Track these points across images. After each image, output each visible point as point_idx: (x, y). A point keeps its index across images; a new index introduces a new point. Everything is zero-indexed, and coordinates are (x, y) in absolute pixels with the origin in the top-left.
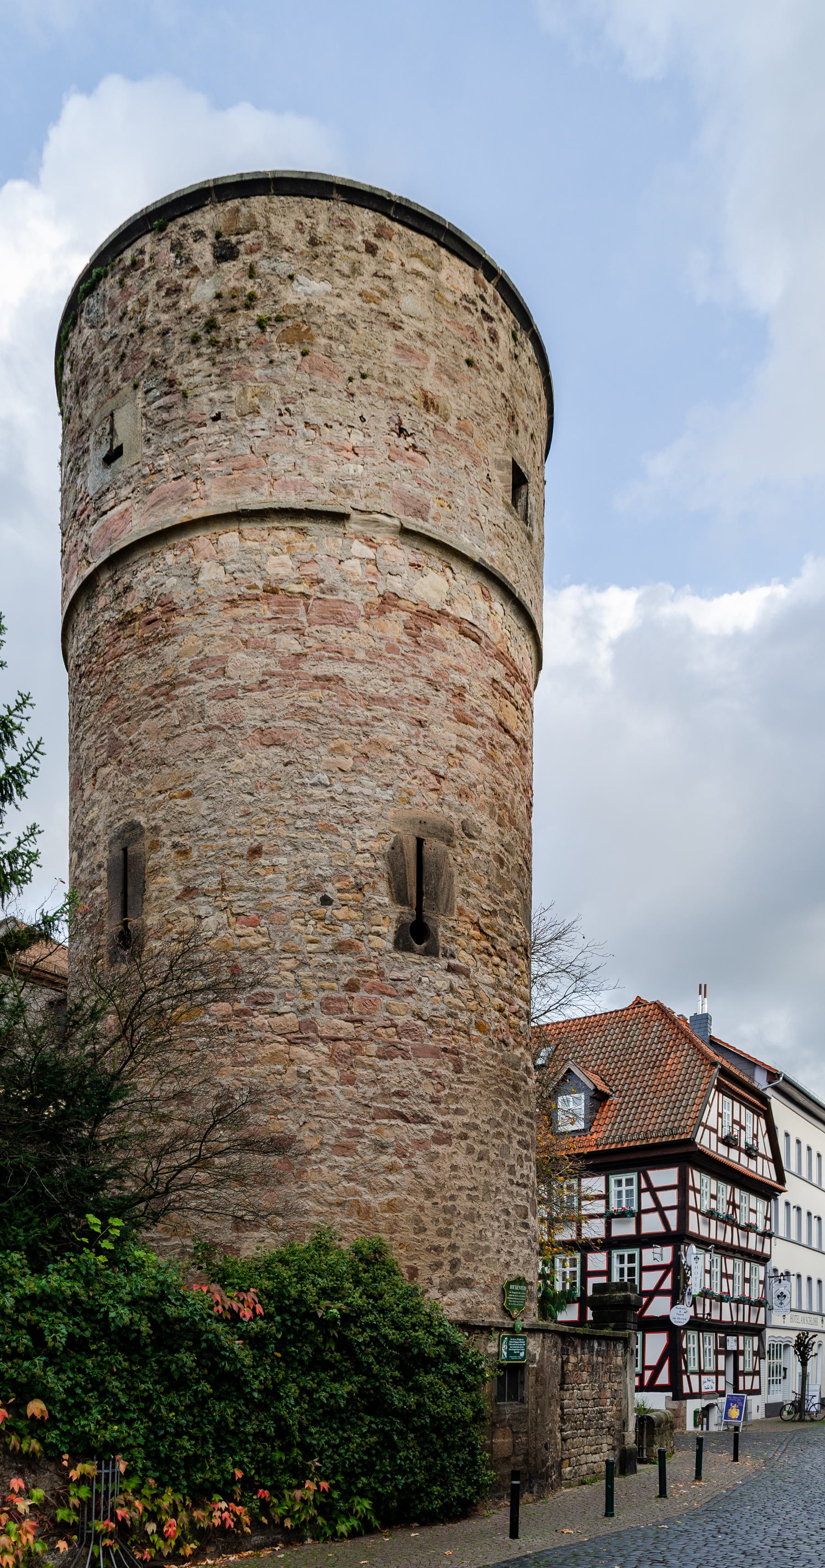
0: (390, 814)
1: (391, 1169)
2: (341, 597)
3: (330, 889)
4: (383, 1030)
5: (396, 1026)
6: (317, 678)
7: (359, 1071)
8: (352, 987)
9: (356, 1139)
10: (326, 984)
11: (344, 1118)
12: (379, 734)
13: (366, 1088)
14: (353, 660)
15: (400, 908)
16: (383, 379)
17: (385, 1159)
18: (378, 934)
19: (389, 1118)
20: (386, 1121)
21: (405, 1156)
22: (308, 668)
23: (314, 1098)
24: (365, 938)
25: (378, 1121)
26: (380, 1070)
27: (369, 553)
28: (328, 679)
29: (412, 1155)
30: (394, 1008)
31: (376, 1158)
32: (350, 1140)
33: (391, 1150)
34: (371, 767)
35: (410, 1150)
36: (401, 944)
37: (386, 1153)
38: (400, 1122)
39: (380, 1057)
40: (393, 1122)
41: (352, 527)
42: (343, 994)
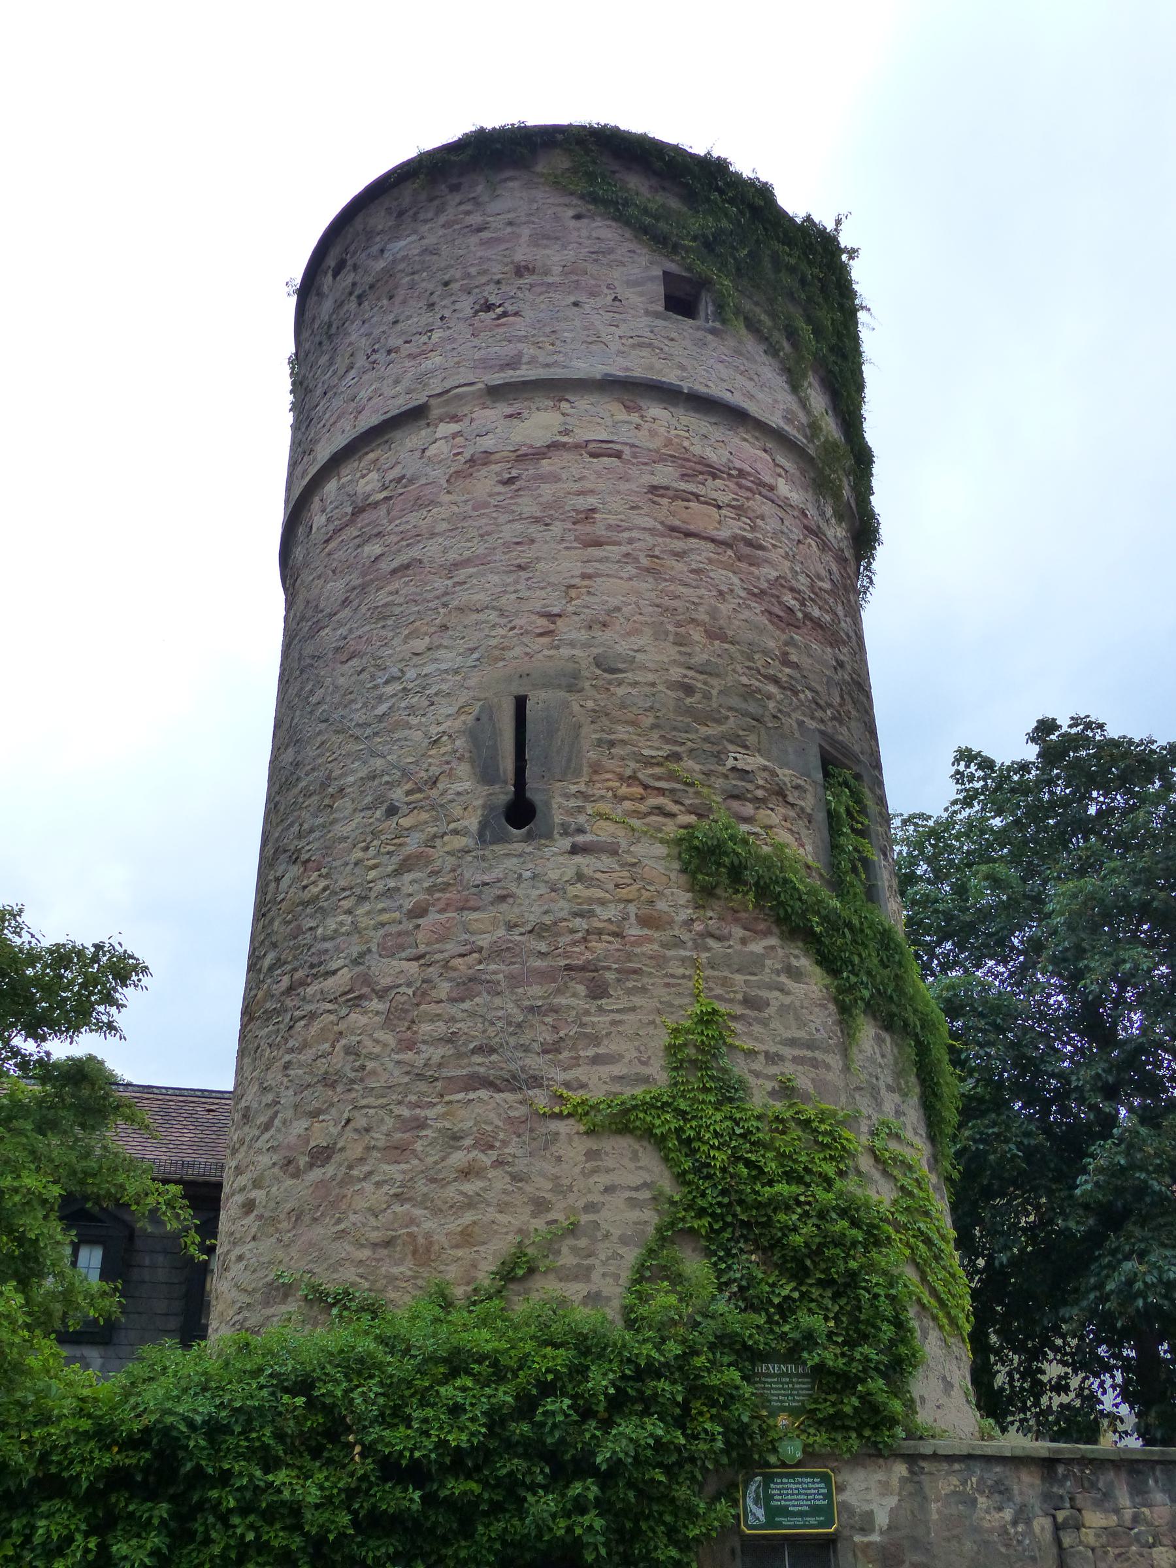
1: (466, 1173)
2: (423, 481)
3: (398, 795)
4: (460, 960)
5: (480, 950)
6: (394, 572)
7: (425, 1028)
8: (419, 912)
9: (415, 1133)
10: (385, 917)
11: (400, 1103)
12: (462, 597)
13: (431, 1050)
14: (433, 535)
15: (484, 790)
16: (468, 276)
17: (458, 1158)
18: (455, 832)
19: (467, 1089)
21: (492, 1147)
22: (385, 566)
23: (362, 1080)
24: (438, 842)
25: (447, 1098)
26: (453, 1019)
27: (454, 427)
28: (407, 567)
29: (505, 1143)
30: (475, 926)
31: (443, 1159)
32: (406, 1136)
33: (468, 1142)
34: (451, 637)
35: (502, 1136)
36: (487, 835)
37: (459, 1148)
38: (483, 1094)
39: (453, 1000)
40: (472, 1095)
41: (435, 413)
42: (408, 925)
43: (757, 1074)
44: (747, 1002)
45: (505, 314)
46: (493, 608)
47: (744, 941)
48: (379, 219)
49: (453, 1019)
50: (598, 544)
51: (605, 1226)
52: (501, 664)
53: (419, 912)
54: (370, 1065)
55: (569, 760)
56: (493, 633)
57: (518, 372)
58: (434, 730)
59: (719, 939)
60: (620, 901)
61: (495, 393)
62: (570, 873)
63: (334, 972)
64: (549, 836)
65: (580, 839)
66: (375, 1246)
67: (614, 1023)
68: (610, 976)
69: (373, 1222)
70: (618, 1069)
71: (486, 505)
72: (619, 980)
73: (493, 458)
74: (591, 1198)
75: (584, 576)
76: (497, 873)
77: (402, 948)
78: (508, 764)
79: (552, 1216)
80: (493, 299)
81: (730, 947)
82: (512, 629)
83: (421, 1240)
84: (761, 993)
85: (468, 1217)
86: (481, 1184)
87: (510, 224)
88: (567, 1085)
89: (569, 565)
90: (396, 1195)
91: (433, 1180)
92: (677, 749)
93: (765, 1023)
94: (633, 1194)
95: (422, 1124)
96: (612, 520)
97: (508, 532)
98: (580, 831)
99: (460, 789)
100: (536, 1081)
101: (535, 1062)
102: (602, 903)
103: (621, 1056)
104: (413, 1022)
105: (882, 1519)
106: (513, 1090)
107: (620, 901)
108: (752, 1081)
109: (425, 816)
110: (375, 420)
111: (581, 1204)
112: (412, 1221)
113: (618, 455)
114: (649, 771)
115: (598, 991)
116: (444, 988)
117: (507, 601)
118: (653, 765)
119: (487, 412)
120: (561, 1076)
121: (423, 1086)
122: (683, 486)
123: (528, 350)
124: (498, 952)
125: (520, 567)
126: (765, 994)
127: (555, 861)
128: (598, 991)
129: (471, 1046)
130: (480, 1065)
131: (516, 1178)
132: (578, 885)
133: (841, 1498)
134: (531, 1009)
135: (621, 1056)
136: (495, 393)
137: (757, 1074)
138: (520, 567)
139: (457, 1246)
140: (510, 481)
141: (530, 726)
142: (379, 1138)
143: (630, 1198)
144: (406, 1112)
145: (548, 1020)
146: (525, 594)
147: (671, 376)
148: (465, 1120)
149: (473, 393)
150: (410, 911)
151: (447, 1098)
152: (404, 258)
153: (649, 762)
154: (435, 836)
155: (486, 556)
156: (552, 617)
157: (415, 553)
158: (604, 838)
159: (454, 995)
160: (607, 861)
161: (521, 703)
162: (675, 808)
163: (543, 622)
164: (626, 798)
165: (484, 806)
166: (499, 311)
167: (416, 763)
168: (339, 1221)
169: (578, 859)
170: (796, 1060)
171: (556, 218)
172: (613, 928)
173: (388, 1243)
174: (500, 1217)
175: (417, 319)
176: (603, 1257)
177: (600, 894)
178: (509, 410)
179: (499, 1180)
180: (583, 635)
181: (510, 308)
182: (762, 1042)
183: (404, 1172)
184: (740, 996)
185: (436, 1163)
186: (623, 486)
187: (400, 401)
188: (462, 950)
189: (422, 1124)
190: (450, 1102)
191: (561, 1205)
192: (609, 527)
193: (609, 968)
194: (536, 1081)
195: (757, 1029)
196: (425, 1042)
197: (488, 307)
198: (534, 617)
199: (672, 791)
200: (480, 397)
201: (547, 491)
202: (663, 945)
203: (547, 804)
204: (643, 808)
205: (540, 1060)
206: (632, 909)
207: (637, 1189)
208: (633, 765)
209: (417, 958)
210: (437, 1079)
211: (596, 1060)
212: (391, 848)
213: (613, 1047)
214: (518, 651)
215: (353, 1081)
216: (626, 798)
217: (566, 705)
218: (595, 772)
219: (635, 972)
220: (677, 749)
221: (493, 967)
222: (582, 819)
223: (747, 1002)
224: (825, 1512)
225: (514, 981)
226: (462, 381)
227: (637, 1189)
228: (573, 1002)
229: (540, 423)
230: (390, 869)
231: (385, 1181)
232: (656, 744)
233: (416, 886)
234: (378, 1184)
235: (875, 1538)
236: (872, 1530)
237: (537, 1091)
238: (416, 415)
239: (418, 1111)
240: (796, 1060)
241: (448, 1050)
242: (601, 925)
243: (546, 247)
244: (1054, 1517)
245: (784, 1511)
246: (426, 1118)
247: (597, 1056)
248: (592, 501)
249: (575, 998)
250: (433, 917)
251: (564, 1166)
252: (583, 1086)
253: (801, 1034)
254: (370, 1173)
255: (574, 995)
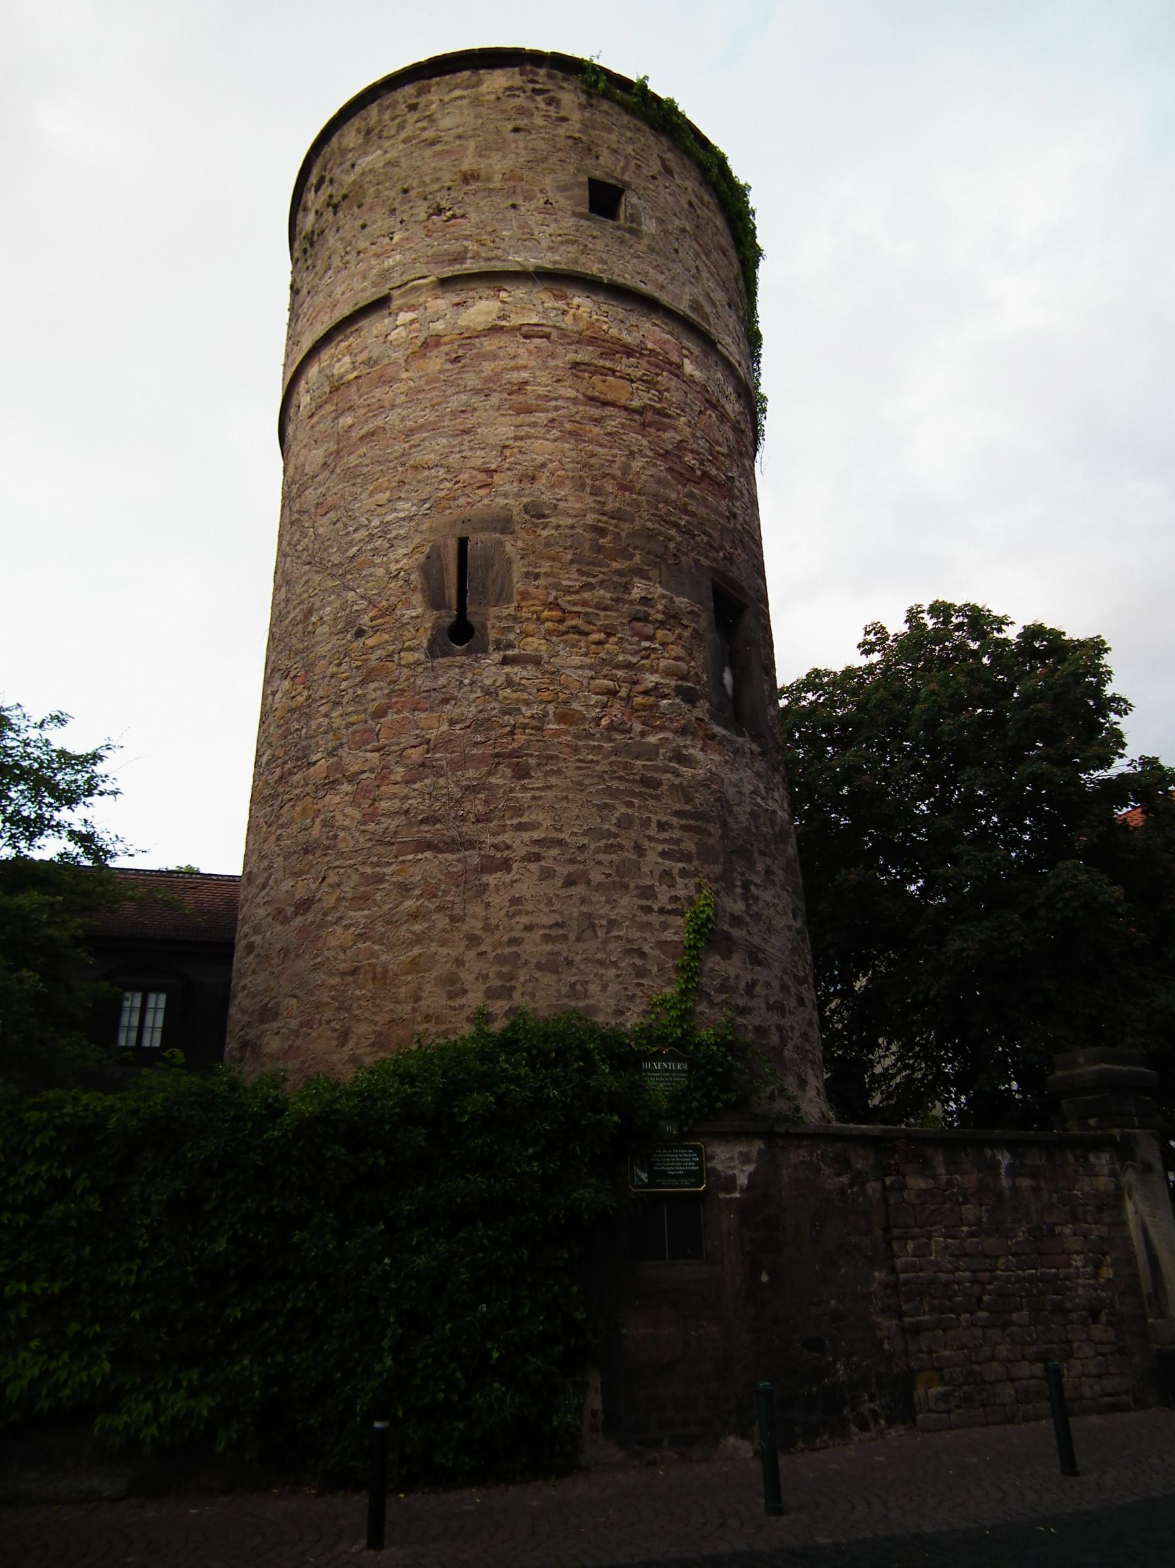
0: (424, 527)
1: (415, 916)
2: (386, 362)
4: (413, 750)
5: (428, 742)
6: (362, 438)
8: (380, 713)
12: (417, 457)
13: (389, 821)
14: (393, 406)
15: (433, 615)
17: (409, 904)
19: (416, 852)
20: (410, 857)
21: (435, 896)
22: (356, 434)
25: (400, 859)
27: (411, 316)
29: (446, 893)
36: (435, 650)
37: (410, 897)
38: (428, 854)
39: (407, 782)
40: (420, 856)
41: (395, 304)
43: (650, 839)
44: (644, 781)
45: (454, 216)
46: (442, 466)
47: (643, 734)
48: (350, 137)
49: (407, 797)
50: (529, 411)
51: (524, 956)
52: (448, 511)
53: (380, 713)
54: (341, 834)
55: (502, 589)
56: (442, 487)
57: (464, 266)
58: (393, 567)
59: (623, 732)
60: (542, 702)
61: (445, 283)
62: (501, 680)
63: (315, 763)
64: (485, 651)
65: (510, 652)
66: (343, 974)
67: (534, 798)
68: (533, 761)
69: (342, 956)
70: (536, 835)
71: (436, 380)
72: (539, 764)
73: (443, 340)
74: (513, 934)
75: (516, 438)
76: (442, 681)
77: (367, 742)
78: (452, 593)
79: (482, 948)
80: (444, 204)
81: (631, 738)
82: (457, 482)
83: (379, 969)
84: (654, 775)
85: (416, 951)
86: (426, 925)
87: (459, 137)
88: (495, 847)
89: (504, 430)
90: (360, 935)
91: (389, 923)
92: (592, 580)
93: (657, 798)
94: (547, 931)
95: (381, 879)
96: (541, 390)
97: (455, 402)
98: (510, 645)
99: (414, 614)
100: (470, 844)
101: (469, 829)
102: (528, 703)
103: (540, 824)
104: (375, 800)
105: (742, 1180)
106: (452, 852)
107: (542, 702)
108: (646, 843)
109: (386, 637)
110: (346, 311)
111: (505, 939)
112: (373, 955)
113: (547, 336)
114: (568, 598)
115: (521, 773)
116: (399, 773)
117: (454, 459)
118: (570, 593)
119: (438, 301)
120: (490, 840)
121: (380, 849)
122: (601, 362)
123: (472, 246)
124: (445, 743)
125: (464, 432)
126: (659, 776)
127: (490, 670)
128: (521, 773)
129: (420, 818)
130: (426, 832)
131: (453, 919)
132: (508, 690)
133: (709, 1165)
134: (468, 788)
135: (540, 824)
136: (445, 283)
137: (650, 839)
138: (464, 432)
139: (407, 973)
140: (457, 359)
141: (470, 561)
142: (347, 890)
143: (545, 935)
144: (369, 870)
145: (482, 796)
146: (467, 453)
147: (594, 269)
148: (415, 875)
149: (426, 285)
150: (373, 713)
151: (400, 859)
152: (371, 171)
153: (568, 591)
154: (393, 652)
155: (436, 423)
156: (490, 472)
157: (379, 422)
158: (529, 651)
159: (407, 778)
160: (531, 671)
161: (463, 543)
162: (586, 628)
163: (481, 477)
164: (547, 620)
165: (433, 628)
166: (449, 214)
167: (379, 594)
168: (317, 956)
169: (507, 669)
170: (683, 828)
171: (498, 132)
172: (534, 723)
173: (354, 972)
174: (440, 950)
175: (380, 222)
176: (522, 979)
177: (525, 696)
178: (456, 300)
179: (442, 922)
180: (515, 487)
181: (459, 212)
182: (656, 813)
183: (366, 917)
184: (638, 778)
185: (391, 909)
186: (552, 363)
187: (368, 294)
188: (413, 742)
189: (381, 879)
190: (404, 862)
191: (489, 940)
192: (539, 397)
193: (531, 755)
194: (470, 844)
195: (650, 803)
196: (383, 815)
197: (439, 211)
198: (475, 473)
199: (586, 614)
200: (433, 289)
201: (488, 367)
202: (577, 737)
203: (484, 626)
204: (563, 628)
205: (474, 828)
206: (551, 708)
207: (550, 927)
208: (554, 593)
209: (378, 750)
210: (393, 844)
211: (520, 827)
212: (360, 663)
213: (533, 817)
214: (462, 501)
215: (328, 848)
216: (547, 620)
217: (500, 544)
218: (523, 599)
219: (552, 757)
220: (592, 580)
221: (438, 755)
222: (511, 636)
223: (644, 781)
224: (696, 1176)
225: (455, 766)
226: (418, 275)
227: (550, 927)
228: (500, 781)
229: (483, 309)
230: (358, 679)
231: (351, 925)
232: (575, 576)
233: (379, 692)
234: (347, 927)
235: (737, 1195)
236: (735, 1190)
237: (471, 852)
238: (381, 304)
239: (378, 869)
240: (683, 828)
241: (402, 821)
242: (527, 721)
243: (488, 157)
244: (883, 1181)
245: (664, 1174)
246: (384, 874)
247: (520, 823)
248: (525, 375)
249: (501, 779)
250: (391, 717)
251: (492, 909)
252: (508, 847)
253: (688, 807)
254: (341, 918)
255: (503, 777)
